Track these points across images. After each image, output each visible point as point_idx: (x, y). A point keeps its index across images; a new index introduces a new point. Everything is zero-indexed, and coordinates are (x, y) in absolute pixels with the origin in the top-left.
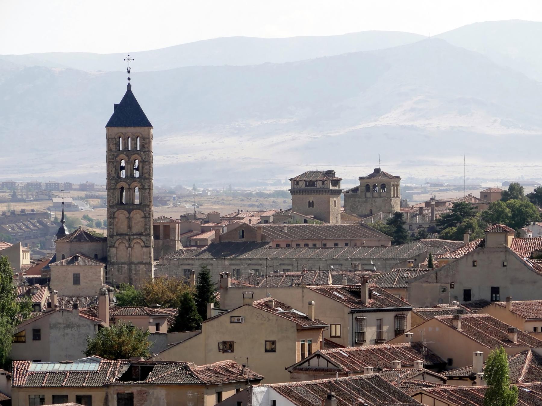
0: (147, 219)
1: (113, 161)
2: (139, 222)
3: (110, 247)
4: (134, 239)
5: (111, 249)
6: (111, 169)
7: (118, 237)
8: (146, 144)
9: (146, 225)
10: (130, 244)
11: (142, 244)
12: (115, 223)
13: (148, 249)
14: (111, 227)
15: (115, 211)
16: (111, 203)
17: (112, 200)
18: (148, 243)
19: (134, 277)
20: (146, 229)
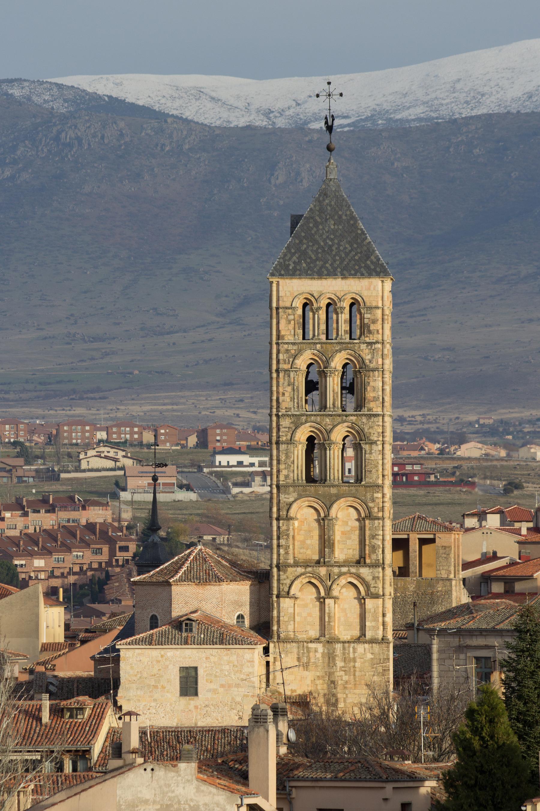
4: (340, 575)
7: (300, 570)
15: (292, 499)
19: (341, 676)
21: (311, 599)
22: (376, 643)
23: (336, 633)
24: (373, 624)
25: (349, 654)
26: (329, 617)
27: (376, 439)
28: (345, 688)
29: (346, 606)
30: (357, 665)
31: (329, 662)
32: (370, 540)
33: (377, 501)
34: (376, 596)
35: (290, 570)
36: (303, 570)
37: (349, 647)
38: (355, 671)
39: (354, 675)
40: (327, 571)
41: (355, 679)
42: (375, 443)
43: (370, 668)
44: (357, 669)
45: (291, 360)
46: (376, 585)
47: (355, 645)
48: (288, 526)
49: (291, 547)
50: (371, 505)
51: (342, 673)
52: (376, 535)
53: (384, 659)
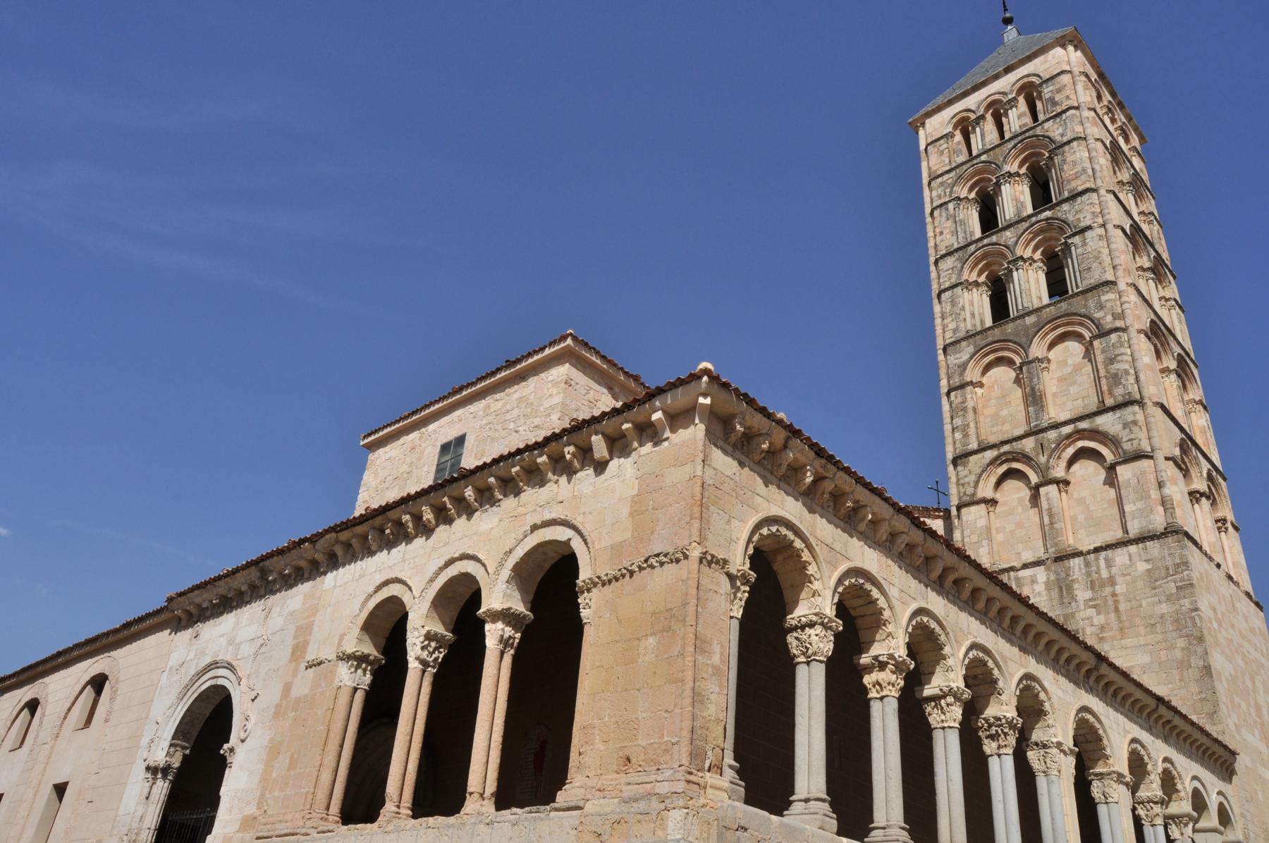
0: (1114, 337)
3: (959, 508)
5: (964, 511)
7: (990, 454)
8: (1059, 91)
9: (1111, 361)
12: (970, 404)
13: (1145, 463)
15: (965, 357)
17: (952, 326)
20: (1115, 379)
21: (1020, 499)
22: (1153, 537)
24: (1140, 505)
26: (1051, 516)
28: (1101, 639)
29: (1085, 493)
31: (1061, 596)
32: (1106, 367)
33: (1108, 305)
34: (1138, 456)
35: (973, 459)
37: (1097, 559)
38: (1116, 602)
39: (1117, 610)
40: (1037, 440)
41: (1119, 618)
42: (1089, 228)
43: (1148, 590)
44: (1121, 598)
46: (1132, 436)
47: (1109, 552)
49: (972, 425)
50: (1097, 315)
51: (1091, 612)
52: (1117, 356)
53: (1178, 565)
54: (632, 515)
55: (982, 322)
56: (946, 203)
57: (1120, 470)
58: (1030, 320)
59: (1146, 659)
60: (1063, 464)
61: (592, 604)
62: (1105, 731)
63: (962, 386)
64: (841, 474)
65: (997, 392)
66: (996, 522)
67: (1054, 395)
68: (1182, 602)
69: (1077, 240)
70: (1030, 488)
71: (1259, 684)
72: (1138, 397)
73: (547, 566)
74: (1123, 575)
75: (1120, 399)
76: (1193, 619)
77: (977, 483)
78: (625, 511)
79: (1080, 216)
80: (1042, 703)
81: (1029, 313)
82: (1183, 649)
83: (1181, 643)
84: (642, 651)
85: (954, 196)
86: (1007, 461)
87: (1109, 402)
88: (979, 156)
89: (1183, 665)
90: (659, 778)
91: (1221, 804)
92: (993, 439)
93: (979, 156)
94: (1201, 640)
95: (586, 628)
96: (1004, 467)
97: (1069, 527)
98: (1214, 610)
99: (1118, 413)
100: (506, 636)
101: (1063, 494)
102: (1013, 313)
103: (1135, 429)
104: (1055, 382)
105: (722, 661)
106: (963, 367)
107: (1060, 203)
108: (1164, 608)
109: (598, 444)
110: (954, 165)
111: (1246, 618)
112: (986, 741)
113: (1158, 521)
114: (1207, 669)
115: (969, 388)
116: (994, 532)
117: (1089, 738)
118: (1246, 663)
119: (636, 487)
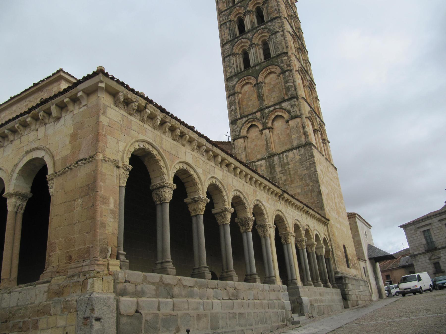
0: (287, 73)
1: (225, 21)
2: (275, 86)
3: (234, 141)
5: (236, 141)
6: (223, 33)
7: (245, 119)
9: (286, 82)
10: (264, 124)
11: (286, 116)
12: (237, 101)
13: (298, 120)
14: (233, 108)
15: (235, 83)
16: (228, 74)
17: (230, 71)
18: (296, 109)
20: (288, 89)
22: (301, 147)
23: (274, 150)
24: (297, 135)
25: (283, 161)
27: (277, 30)
28: (285, 185)
30: (290, 166)
31: (271, 171)
32: (285, 85)
33: (285, 61)
34: (296, 117)
36: (247, 119)
37: (283, 156)
38: (290, 171)
39: (290, 174)
41: (290, 177)
42: (278, 32)
45: (226, 18)
46: (294, 110)
47: (287, 153)
48: (234, 97)
50: (282, 65)
51: (281, 175)
52: (288, 80)
53: (309, 156)
54: (70, 142)
55: (241, 69)
56: (226, 23)
57: (290, 122)
58: (257, 68)
59: (299, 191)
60: (270, 122)
61: (54, 186)
62: (285, 218)
63: (234, 94)
64: (174, 120)
65: (246, 96)
66: (248, 145)
67: (267, 96)
68: (311, 169)
69: (274, 36)
70: (260, 131)
71: (336, 196)
72: (295, 95)
73: (37, 171)
74: (292, 161)
75: (290, 96)
76: (315, 175)
77: (240, 130)
78: (68, 141)
79: (275, 27)
80: (262, 210)
81: (257, 65)
82: (312, 186)
83: (311, 184)
84: (76, 206)
85: (229, 20)
86: (251, 121)
87: (286, 98)
88: (238, 3)
89: (312, 191)
90: (84, 264)
91: (324, 238)
92: (246, 114)
93: (238, 3)
94: (318, 182)
95: (52, 197)
96: (250, 124)
97: (273, 145)
98: (322, 171)
99: (289, 102)
100: (18, 204)
101: (271, 133)
102: (252, 65)
103: (295, 107)
104: (267, 91)
105: (115, 207)
106: (234, 86)
107: (268, 22)
108: (306, 172)
109: (54, 109)
110: (228, 7)
111: (332, 173)
112: (241, 227)
113: (303, 140)
114: (320, 192)
115: (236, 95)
116: (247, 149)
117: (280, 221)
118: (332, 189)
119: (72, 129)
